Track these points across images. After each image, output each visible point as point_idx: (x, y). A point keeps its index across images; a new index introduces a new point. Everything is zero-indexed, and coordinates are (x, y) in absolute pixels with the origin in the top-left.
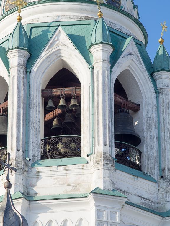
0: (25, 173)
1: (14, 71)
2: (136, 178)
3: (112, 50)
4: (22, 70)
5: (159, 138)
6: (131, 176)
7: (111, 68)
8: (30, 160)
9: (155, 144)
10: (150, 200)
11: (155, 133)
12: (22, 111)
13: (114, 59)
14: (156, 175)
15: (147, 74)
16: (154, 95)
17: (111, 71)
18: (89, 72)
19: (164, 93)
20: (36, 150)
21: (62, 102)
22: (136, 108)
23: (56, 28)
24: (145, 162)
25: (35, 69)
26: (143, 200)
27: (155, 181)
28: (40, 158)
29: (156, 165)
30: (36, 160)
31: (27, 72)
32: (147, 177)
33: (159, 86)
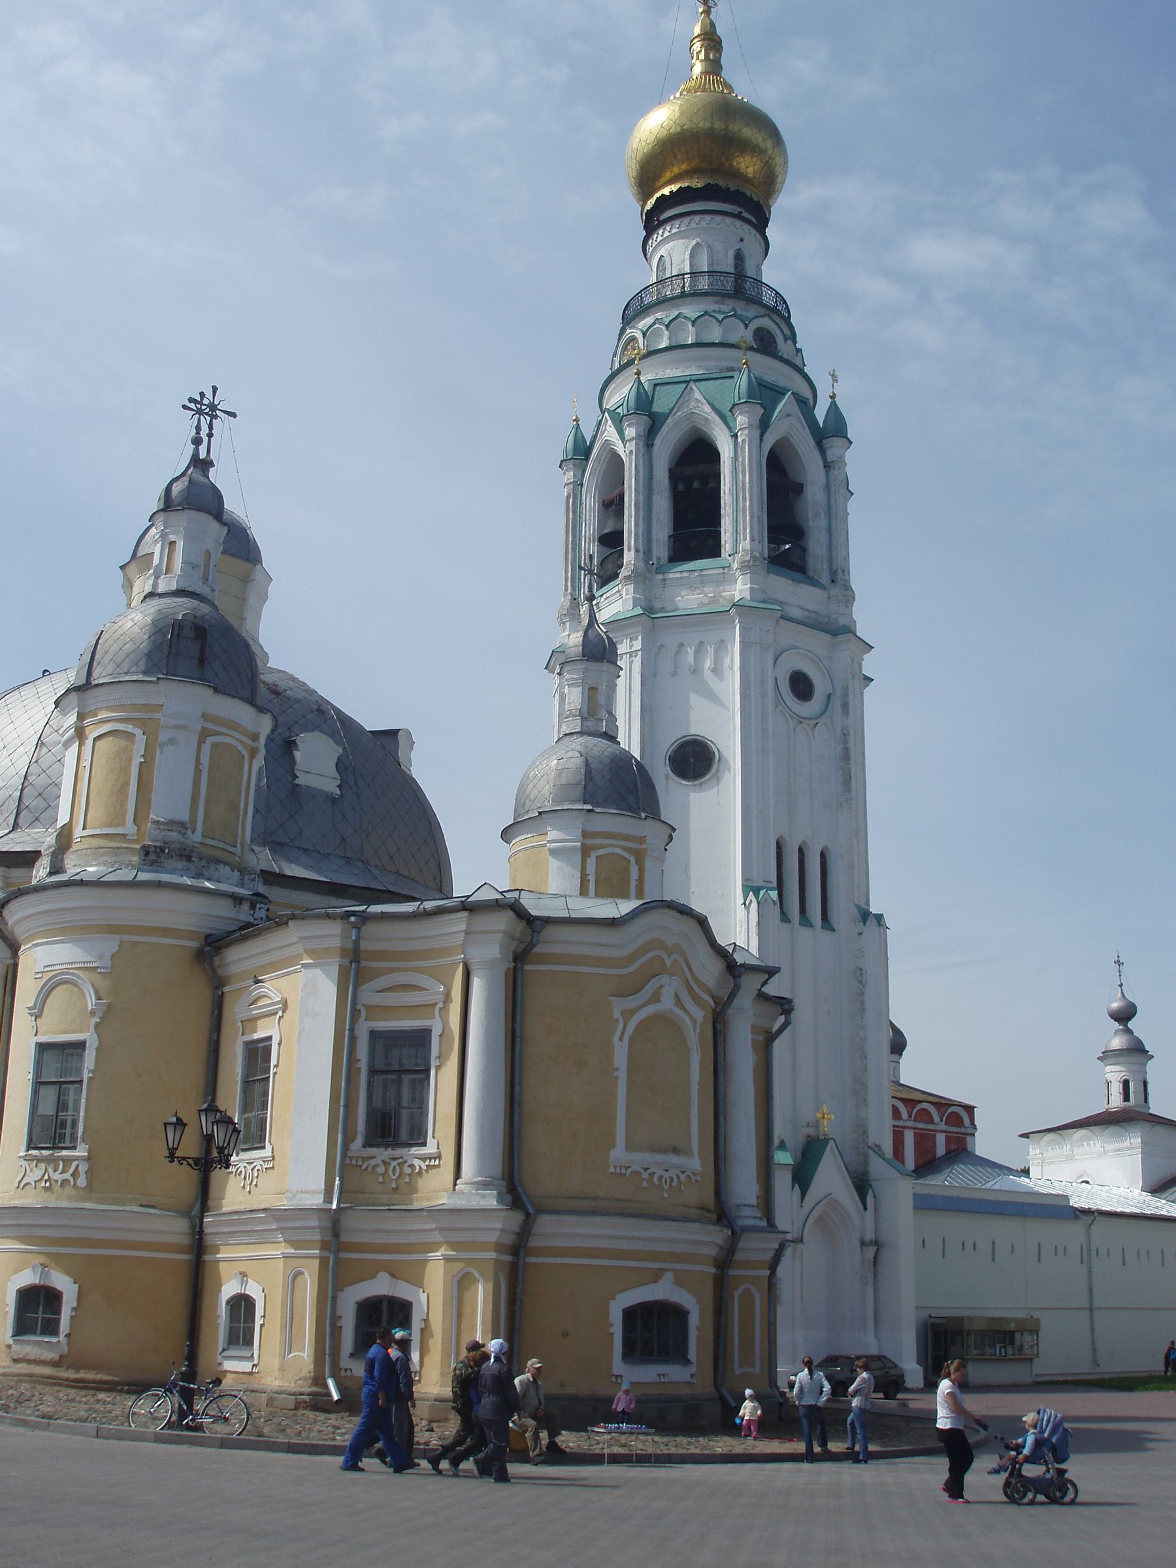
0: (647, 581)
1: (631, 446)
2: (796, 584)
3: (762, 411)
4: (641, 443)
5: (829, 530)
6: (790, 582)
7: (762, 435)
8: (653, 564)
9: (824, 537)
10: (816, 613)
11: (823, 522)
12: (641, 497)
13: (764, 425)
14: (825, 578)
15: (812, 443)
16: (822, 471)
17: (761, 440)
18: (731, 442)
19: (836, 467)
20: (661, 551)
21: (696, 485)
22: (799, 489)
23: (683, 386)
24: (811, 563)
25: (658, 441)
26: (806, 614)
27: (823, 587)
28: (666, 561)
29: (826, 566)
30: (661, 563)
31: (648, 445)
32: (812, 582)
33: (830, 458)
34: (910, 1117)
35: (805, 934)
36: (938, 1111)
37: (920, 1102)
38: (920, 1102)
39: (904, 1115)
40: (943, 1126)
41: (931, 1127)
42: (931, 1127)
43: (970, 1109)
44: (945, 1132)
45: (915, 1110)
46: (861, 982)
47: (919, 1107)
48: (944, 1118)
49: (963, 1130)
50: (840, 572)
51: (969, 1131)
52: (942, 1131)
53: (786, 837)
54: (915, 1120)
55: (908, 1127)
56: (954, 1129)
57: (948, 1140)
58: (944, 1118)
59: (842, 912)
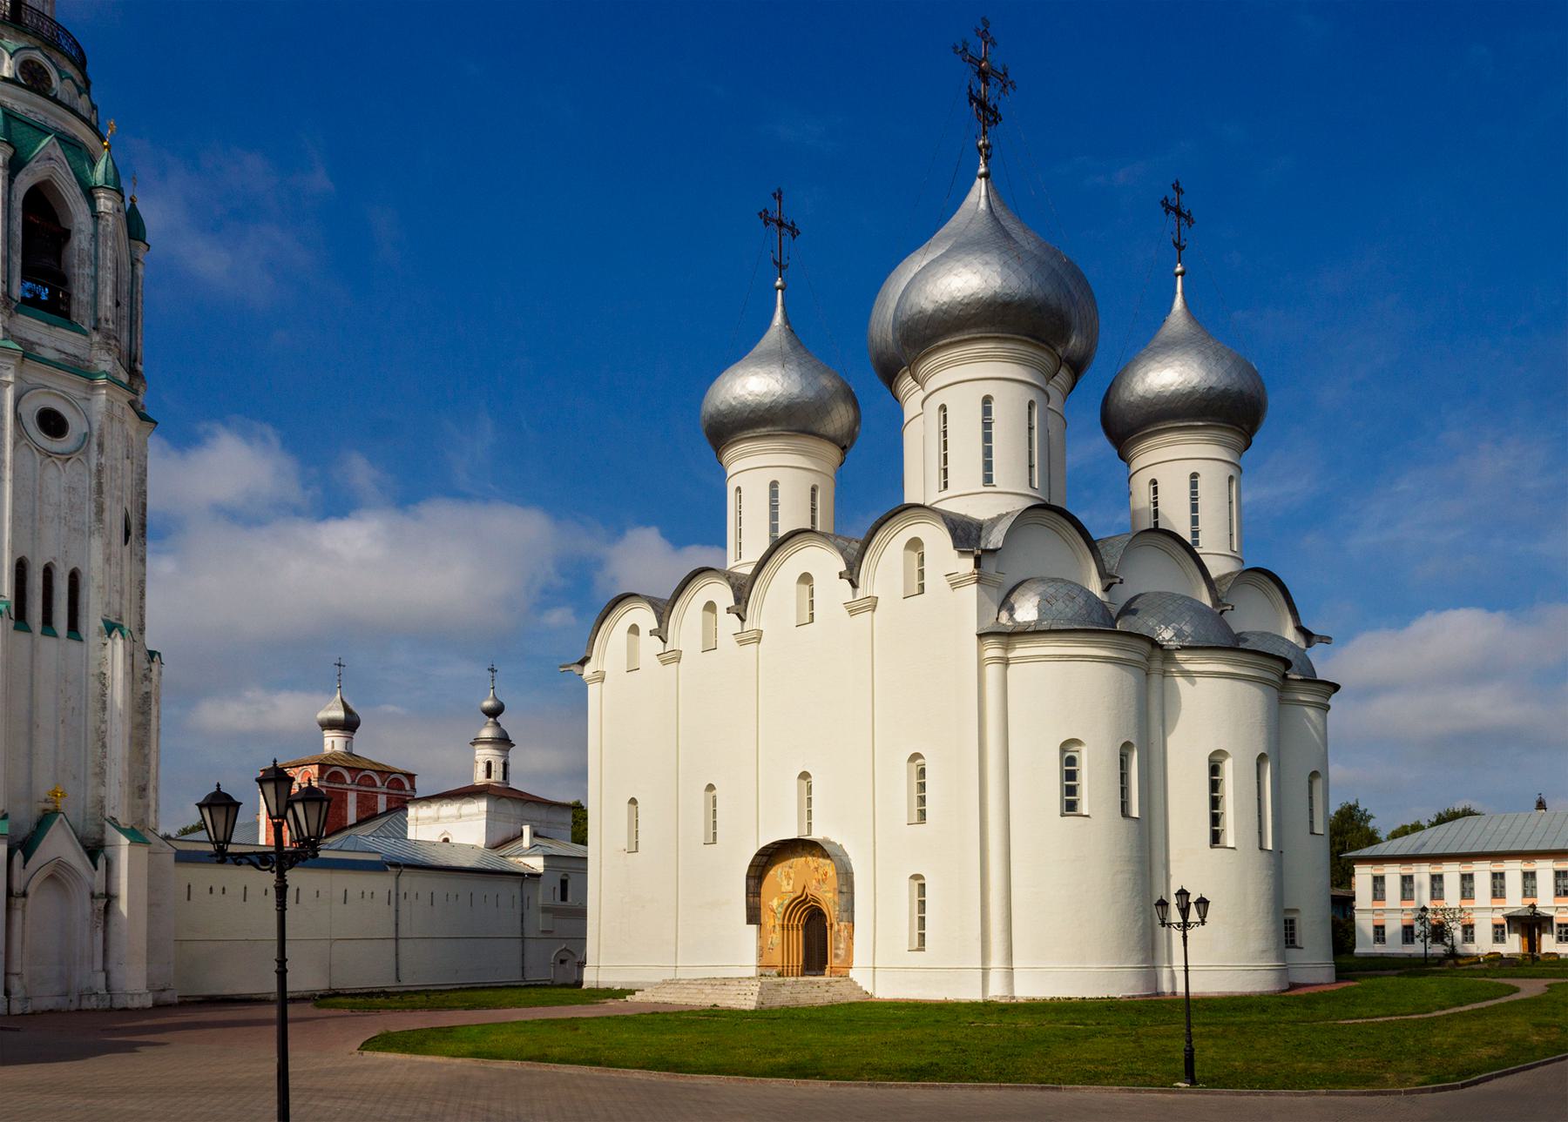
34: (353, 781)
35: (47, 643)
36: (381, 777)
37: (364, 770)
38: (364, 770)
39: (349, 780)
40: (386, 790)
41: (374, 790)
42: (374, 790)
43: (411, 777)
44: (387, 794)
45: (358, 778)
46: (104, 685)
47: (362, 774)
48: (386, 784)
49: (403, 793)
51: (408, 793)
52: (384, 793)
53: (29, 557)
54: (358, 784)
55: (351, 790)
56: (395, 792)
57: (389, 801)
58: (386, 784)
59: (92, 620)
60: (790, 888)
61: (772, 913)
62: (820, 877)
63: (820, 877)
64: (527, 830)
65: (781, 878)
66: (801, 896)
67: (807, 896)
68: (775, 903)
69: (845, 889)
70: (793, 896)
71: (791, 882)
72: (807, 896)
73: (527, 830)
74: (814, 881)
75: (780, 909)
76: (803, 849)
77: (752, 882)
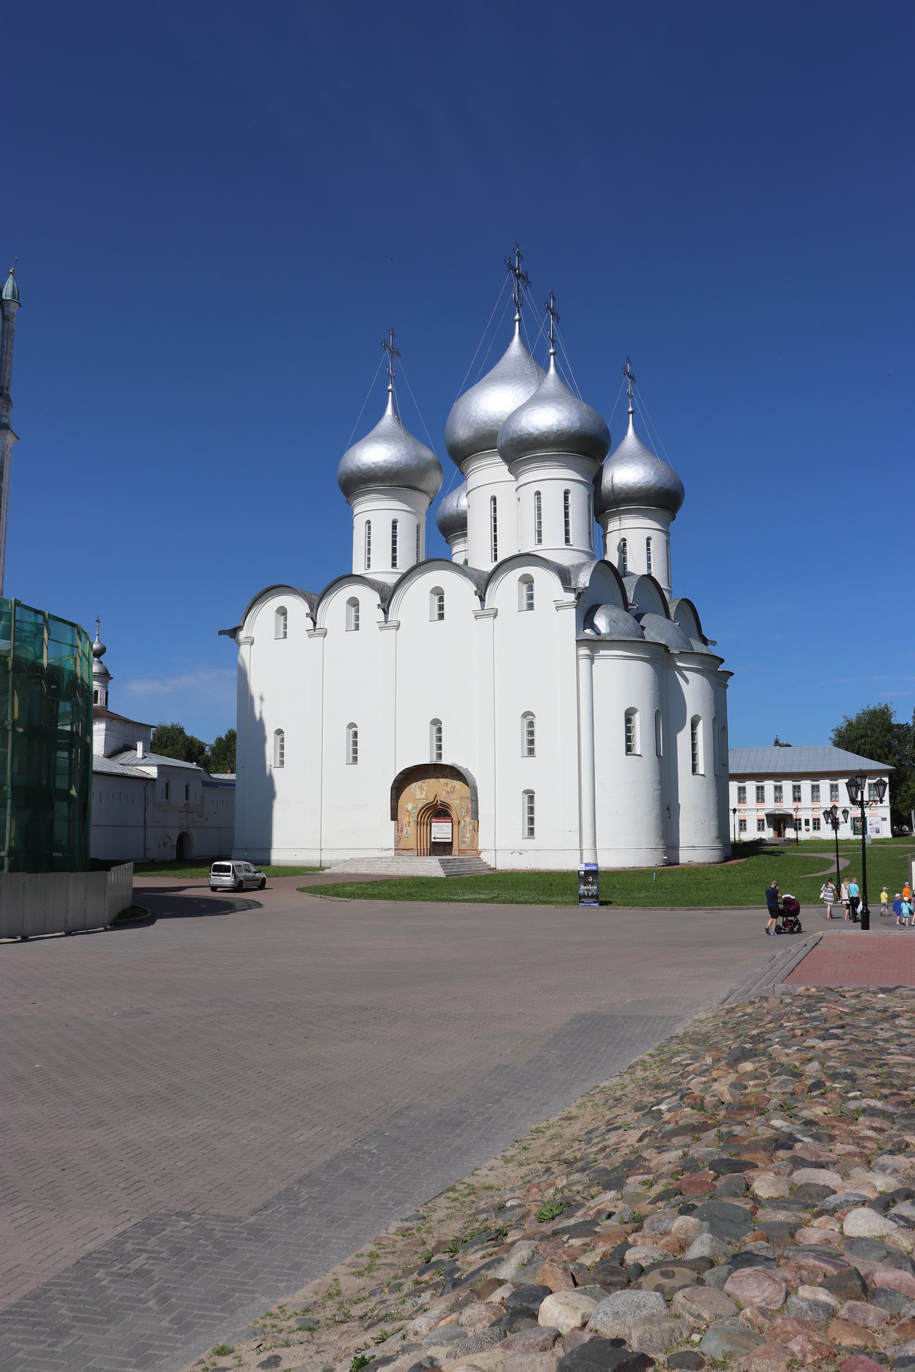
33: (6, 313)
50: (5, 389)
60: (423, 796)
61: (407, 813)
62: (449, 790)
63: (449, 790)
64: (140, 745)
65: (415, 790)
66: (433, 802)
67: (437, 801)
68: (410, 806)
69: (474, 799)
70: (425, 802)
71: (424, 793)
72: (437, 801)
73: (140, 745)
74: (444, 793)
75: (414, 811)
76: (434, 771)
77: (394, 792)
